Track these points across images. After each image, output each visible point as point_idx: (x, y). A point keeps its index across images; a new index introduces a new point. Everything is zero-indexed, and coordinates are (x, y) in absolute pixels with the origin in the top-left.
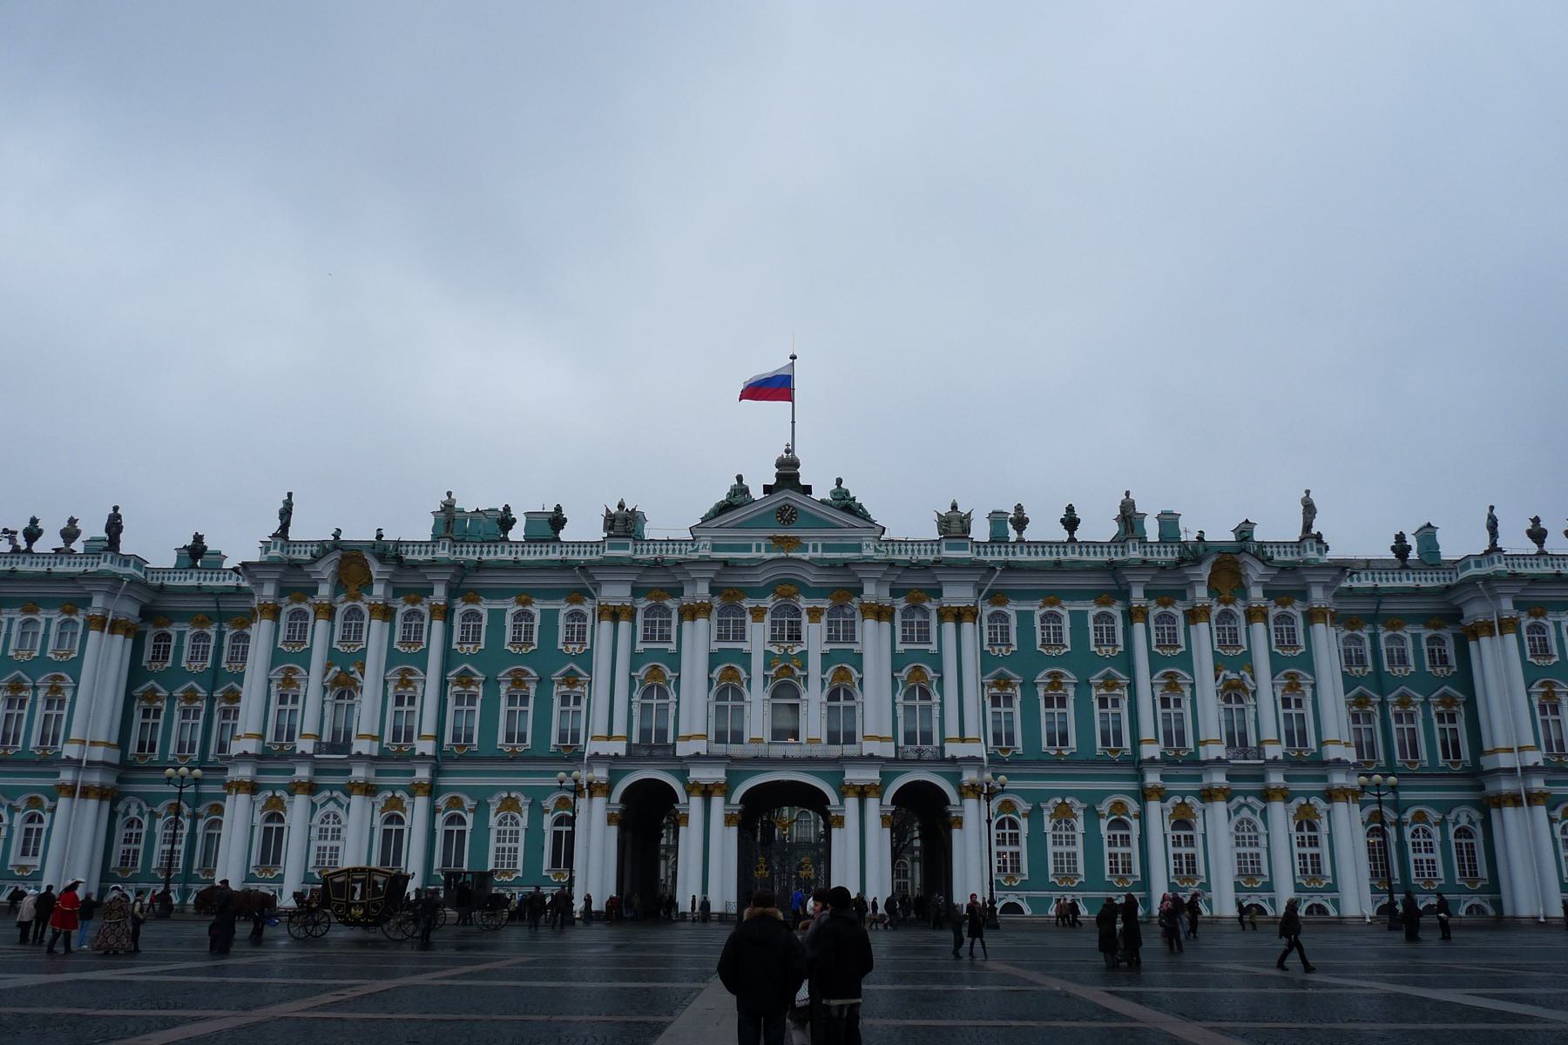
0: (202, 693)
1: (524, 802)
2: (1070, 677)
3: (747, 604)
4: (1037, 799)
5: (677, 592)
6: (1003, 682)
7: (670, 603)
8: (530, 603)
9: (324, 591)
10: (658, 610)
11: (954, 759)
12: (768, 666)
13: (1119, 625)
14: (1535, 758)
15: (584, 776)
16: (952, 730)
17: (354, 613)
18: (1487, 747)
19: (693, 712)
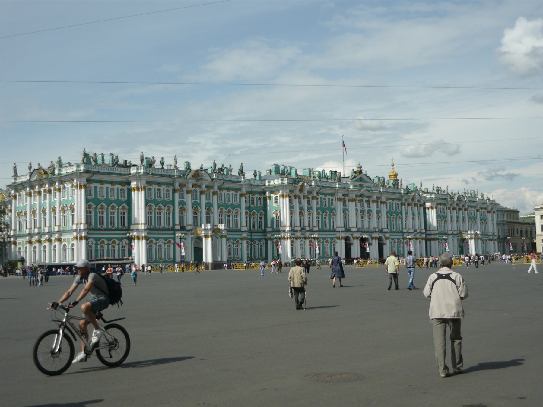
0: (249, 213)
1: (329, 240)
2: (395, 216)
3: (358, 198)
4: (393, 239)
5: (347, 195)
6: (387, 217)
7: (347, 198)
8: (325, 196)
9: (298, 191)
10: (345, 199)
11: (385, 232)
12: (361, 212)
13: (400, 205)
14: (437, 232)
15: (338, 235)
16: (383, 227)
17: (299, 197)
18: (428, 229)
19: (352, 223)
